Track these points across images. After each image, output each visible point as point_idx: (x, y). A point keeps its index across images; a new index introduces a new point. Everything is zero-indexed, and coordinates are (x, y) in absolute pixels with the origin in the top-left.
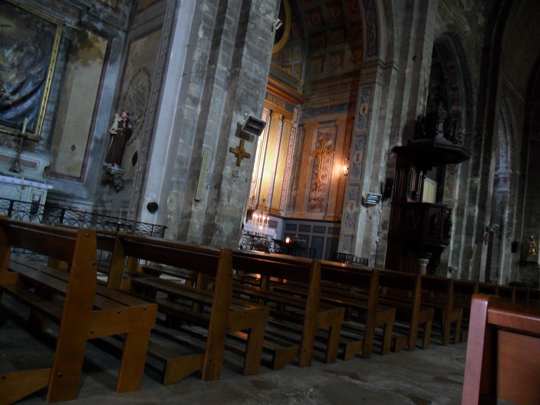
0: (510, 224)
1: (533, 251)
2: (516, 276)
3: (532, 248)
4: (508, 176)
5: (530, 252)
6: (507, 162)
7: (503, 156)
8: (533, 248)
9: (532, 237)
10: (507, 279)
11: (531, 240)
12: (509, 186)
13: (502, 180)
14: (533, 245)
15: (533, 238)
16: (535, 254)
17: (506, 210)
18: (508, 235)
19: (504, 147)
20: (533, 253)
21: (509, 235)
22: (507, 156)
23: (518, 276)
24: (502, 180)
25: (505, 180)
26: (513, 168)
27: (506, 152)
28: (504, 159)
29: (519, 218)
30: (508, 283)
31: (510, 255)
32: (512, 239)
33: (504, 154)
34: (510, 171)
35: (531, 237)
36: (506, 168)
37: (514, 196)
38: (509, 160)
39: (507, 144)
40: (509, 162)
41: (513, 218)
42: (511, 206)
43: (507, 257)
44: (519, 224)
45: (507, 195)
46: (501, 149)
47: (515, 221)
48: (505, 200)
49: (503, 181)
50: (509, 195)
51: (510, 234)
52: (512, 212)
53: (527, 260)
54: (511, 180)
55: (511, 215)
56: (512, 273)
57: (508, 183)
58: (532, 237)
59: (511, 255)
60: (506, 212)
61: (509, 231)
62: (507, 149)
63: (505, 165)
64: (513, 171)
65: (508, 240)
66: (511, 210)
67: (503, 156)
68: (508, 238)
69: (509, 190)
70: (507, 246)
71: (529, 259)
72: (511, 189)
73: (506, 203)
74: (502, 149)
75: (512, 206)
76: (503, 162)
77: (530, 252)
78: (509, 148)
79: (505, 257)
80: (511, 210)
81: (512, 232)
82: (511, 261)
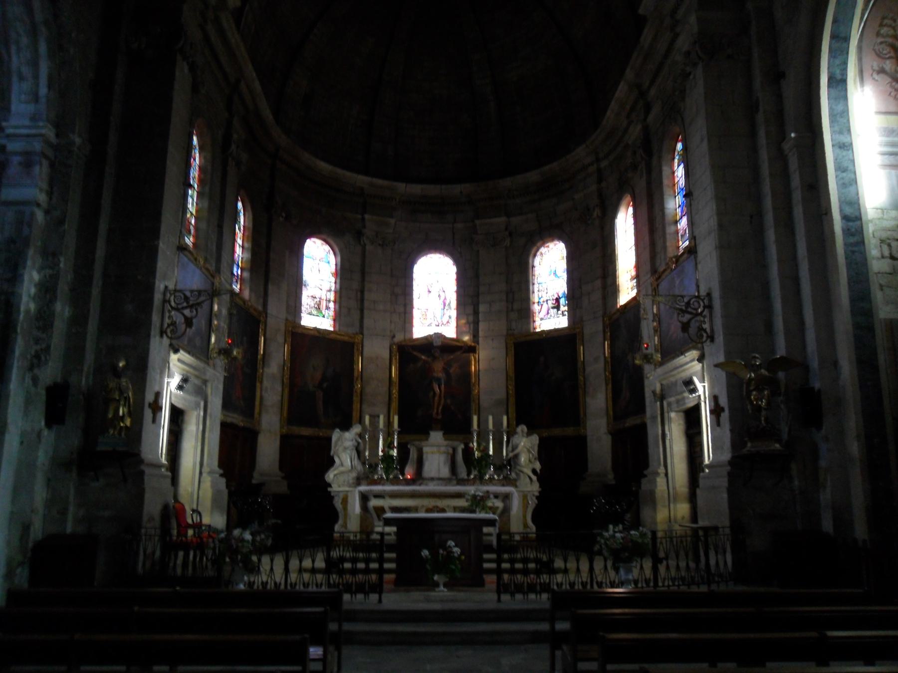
0: (44, 319)
1: (121, 413)
2: (64, 512)
3: (119, 401)
4: (38, 146)
5: (110, 416)
6: (36, 99)
7: (21, 78)
8: (122, 402)
9: (121, 365)
10: (26, 528)
11: (117, 373)
12: (45, 186)
13: (16, 160)
14: (121, 392)
15: (125, 367)
16: (128, 422)
17: (24, 268)
18: (35, 361)
19: (24, 40)
20: (122, 419)
21: (37, 361)
22: (36, 77)
23: (71, 509)
24: (16, 160)
25: (28, 164)
26: (61, 125)
27: (34, 64)
28: (26, 86)
29: (79, 297)
30: (31, 545)
31: (39, 435)
32: (50, 373)
33: (26, 71)
34: (50, 133)
35: (118, 362)
36: (34, 118)
37: (61, 222)
38: (43, 91)
39: (33, 32)
40: (43, 100)
41: (53, 300)
42: (50, 255)
43: (29, 442)
44: (78, 320)
45: (33, 214)
46: (13, 49)
47: (62, 310)
48: (26, 231)
49: (20, 164)
50: (40, 216)
51: (43, 358)
52: (51, 276)
53: (101, 448)
54: (52, 165)
55: (47, 290)
56: (50, 503)
57: (41, 171)
58: (121, 365)
59: (46, 432)
60: (26, 277)
61: (38, 347)
62: (36, 50)
63: (31, 108)
64: (57, 136)
65: (35, 380)
66: (48, 272)
67: (21, 78)
68: (36, 371)
69: (42, 198)
70: (28, 402)
71: (104, 445)
72: (50, 194)
73: (26, 242)
74: (19, 50)
75: (54, 255)
76: (23, 97)
77: (110, 416)
78: (43, 48)
79: (22, 443)
80: (48, 272)
81: (48, 348)
82: (42, 457)
